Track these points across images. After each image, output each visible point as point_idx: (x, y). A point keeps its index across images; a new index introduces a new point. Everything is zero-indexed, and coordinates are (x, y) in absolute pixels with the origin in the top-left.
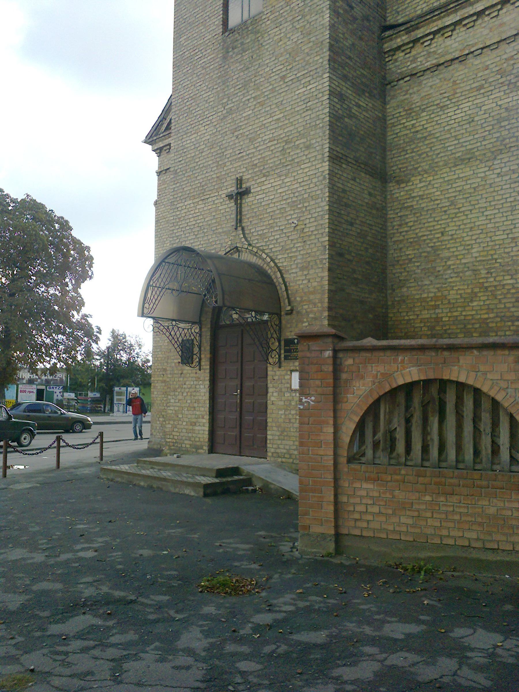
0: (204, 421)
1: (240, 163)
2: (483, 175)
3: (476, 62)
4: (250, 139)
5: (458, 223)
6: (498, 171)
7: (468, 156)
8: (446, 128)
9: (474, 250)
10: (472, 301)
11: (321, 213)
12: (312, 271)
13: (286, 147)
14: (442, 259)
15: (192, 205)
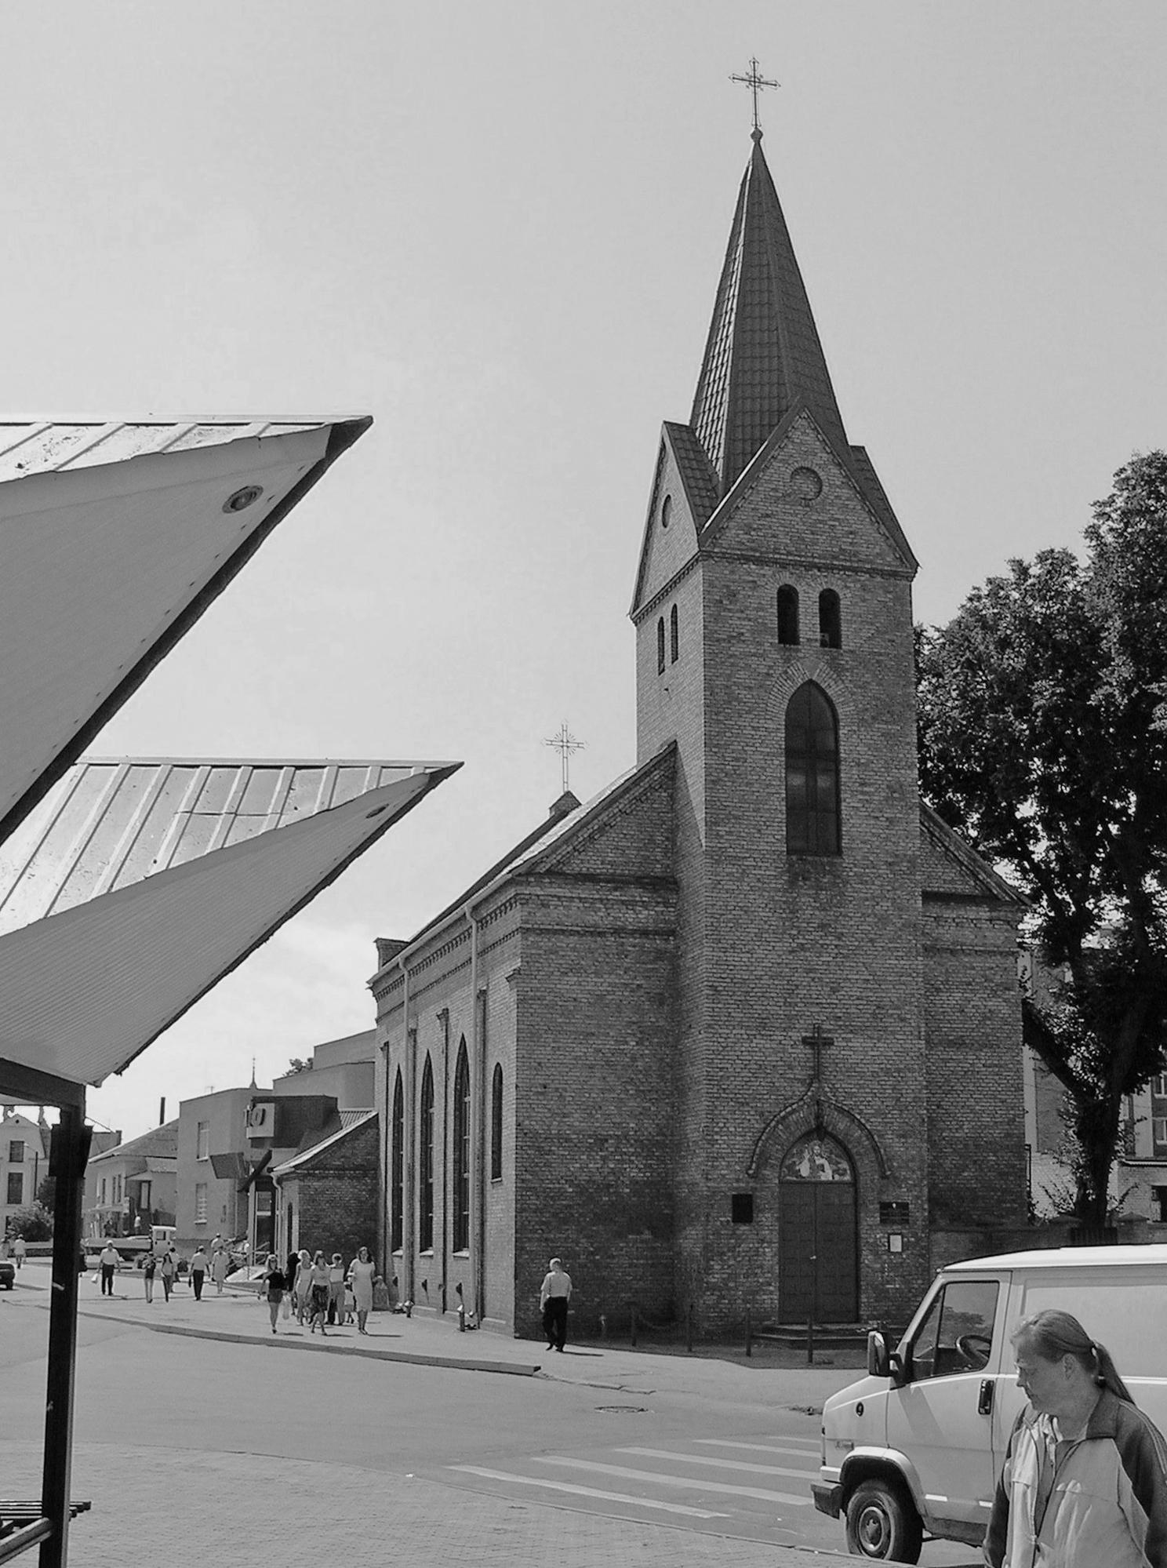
0: (771, 1288)
1: (819, 1010)
2: (971, 1062)
3: (966, 960)
4: (831, 988)
5: (952, 1100)
6: (984, 1062)
7: (961, 1042)
8: (941, 1010)
9: (965, 1127)
10: (963, 1172)
11: (919, 1087)
12: (910, 1141)
13: (877, 1011)
14: (937, 1130)
15: (745, 1037)
